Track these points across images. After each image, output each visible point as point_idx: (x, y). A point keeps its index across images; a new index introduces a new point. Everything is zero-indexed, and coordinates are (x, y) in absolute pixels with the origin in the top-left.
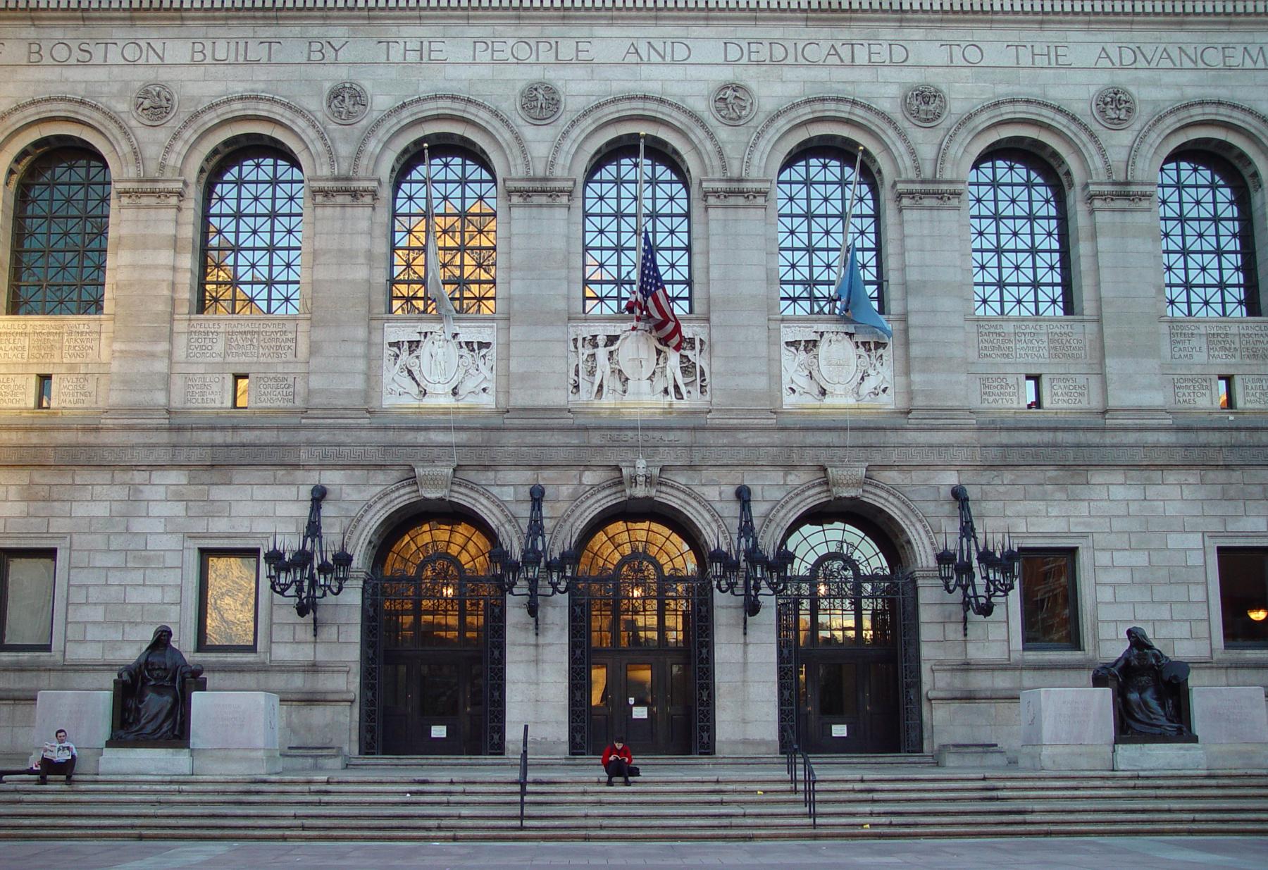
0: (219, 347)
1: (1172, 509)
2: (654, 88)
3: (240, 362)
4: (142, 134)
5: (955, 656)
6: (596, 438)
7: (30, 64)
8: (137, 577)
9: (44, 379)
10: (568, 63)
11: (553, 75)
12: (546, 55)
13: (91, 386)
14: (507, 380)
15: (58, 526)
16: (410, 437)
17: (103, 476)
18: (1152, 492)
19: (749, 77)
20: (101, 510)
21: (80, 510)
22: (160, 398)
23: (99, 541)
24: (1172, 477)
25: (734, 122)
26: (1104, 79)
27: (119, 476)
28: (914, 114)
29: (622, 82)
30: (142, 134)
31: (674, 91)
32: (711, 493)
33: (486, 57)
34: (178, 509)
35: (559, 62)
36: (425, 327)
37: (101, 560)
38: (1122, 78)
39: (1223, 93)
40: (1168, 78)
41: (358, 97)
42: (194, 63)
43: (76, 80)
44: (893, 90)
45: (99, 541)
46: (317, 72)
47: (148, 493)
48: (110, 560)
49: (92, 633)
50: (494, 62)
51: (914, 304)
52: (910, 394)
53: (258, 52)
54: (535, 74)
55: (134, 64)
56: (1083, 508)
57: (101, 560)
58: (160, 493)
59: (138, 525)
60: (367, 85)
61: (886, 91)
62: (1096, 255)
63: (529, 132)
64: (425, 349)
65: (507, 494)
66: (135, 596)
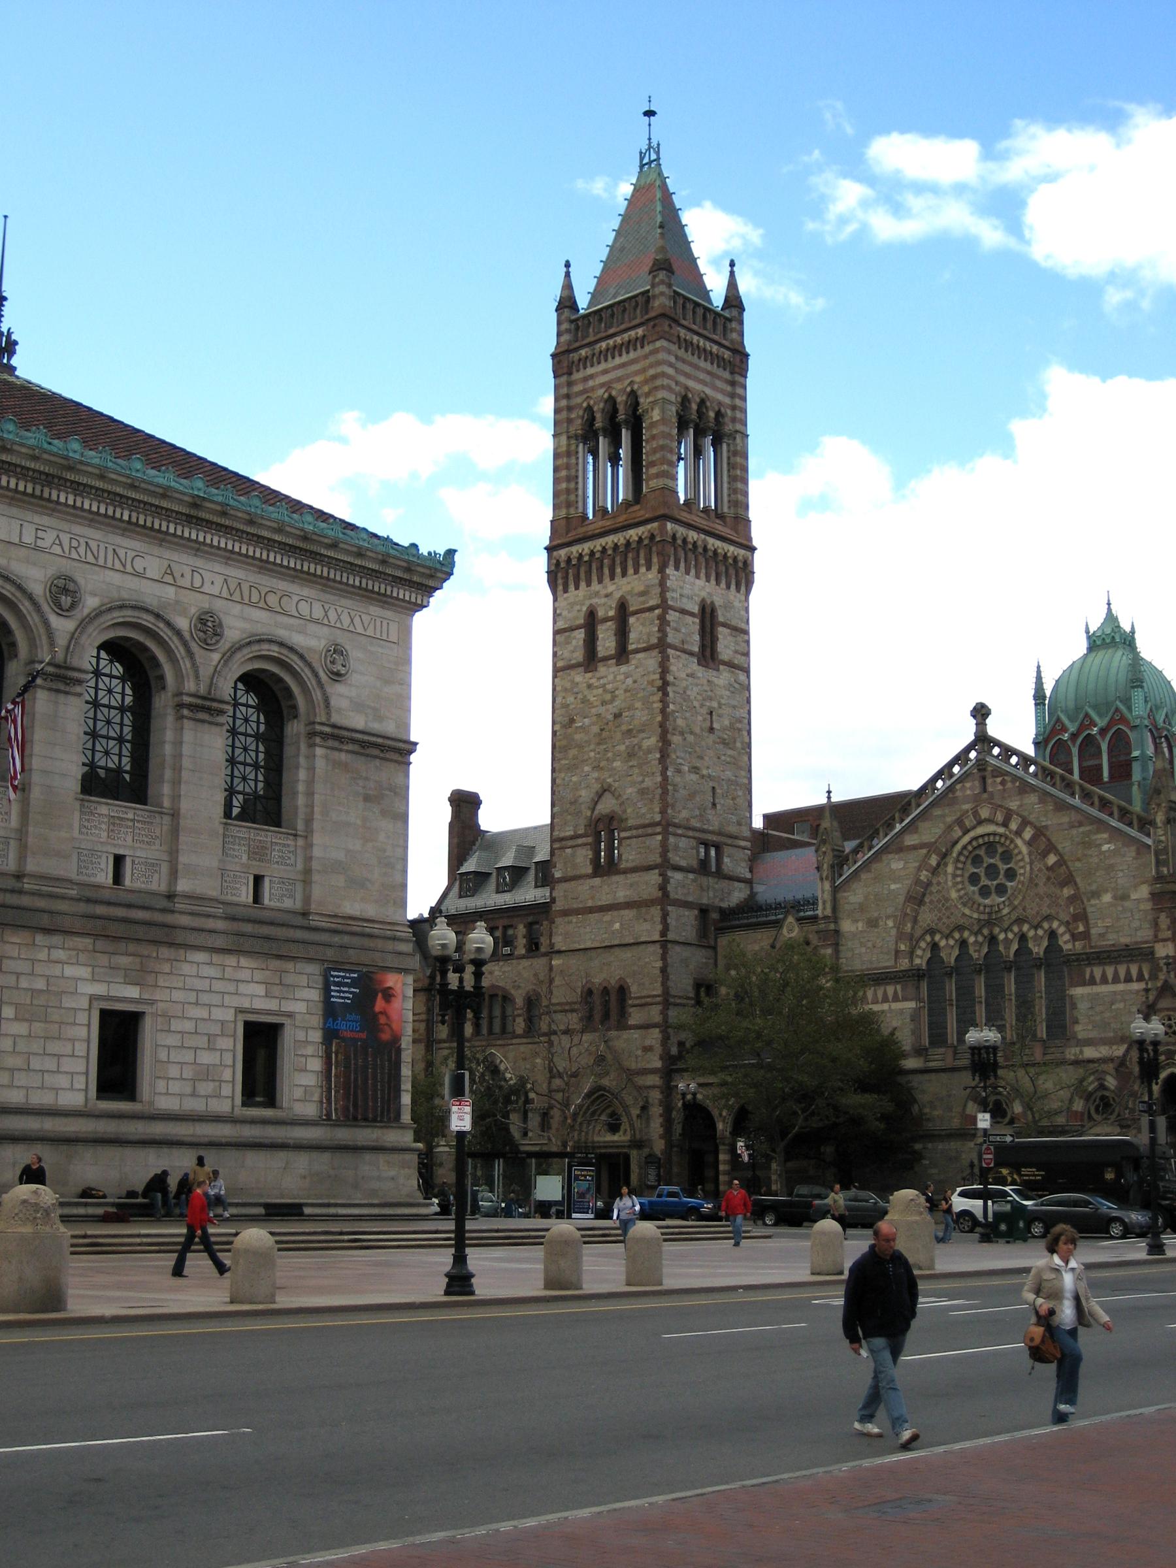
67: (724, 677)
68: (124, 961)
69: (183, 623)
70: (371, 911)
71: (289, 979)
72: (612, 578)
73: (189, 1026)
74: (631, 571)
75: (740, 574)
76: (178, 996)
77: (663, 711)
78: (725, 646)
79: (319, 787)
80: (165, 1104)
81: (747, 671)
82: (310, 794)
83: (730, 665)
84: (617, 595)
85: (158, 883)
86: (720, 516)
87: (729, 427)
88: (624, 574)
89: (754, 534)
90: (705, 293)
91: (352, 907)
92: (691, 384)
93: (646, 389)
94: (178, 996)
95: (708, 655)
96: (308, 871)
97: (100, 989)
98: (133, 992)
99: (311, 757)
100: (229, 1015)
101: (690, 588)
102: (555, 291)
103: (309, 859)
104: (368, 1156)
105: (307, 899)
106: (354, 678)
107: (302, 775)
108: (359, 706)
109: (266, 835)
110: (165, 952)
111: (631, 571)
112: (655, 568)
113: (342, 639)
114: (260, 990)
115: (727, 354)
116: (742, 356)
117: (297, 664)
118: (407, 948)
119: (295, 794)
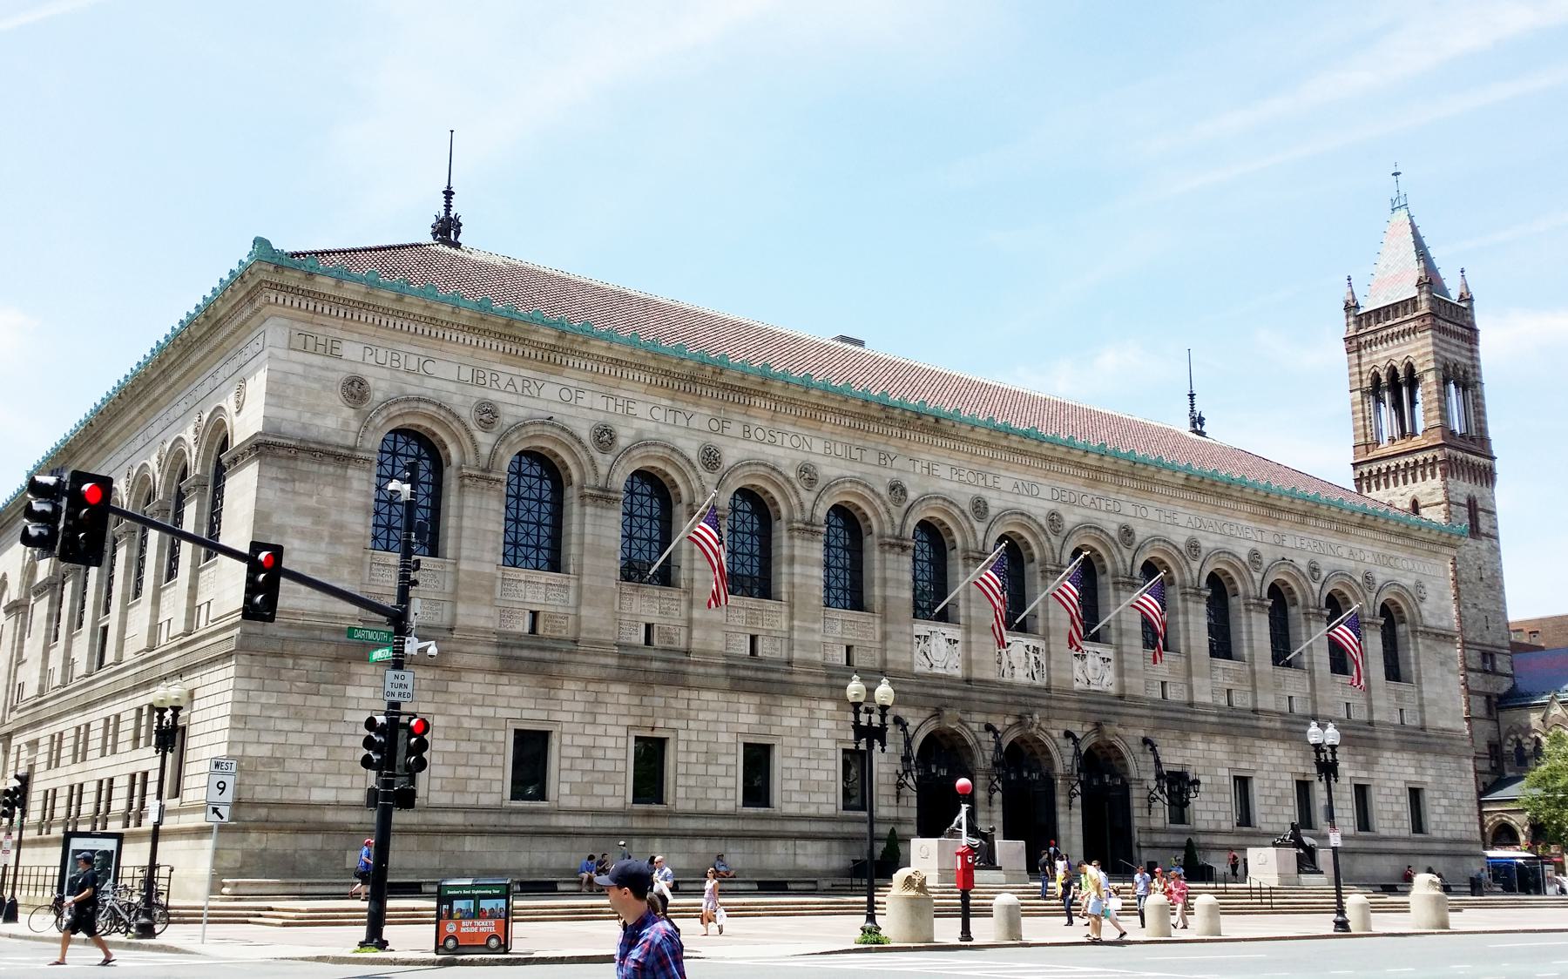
0: (839, 628)
1: (1220, 756)
2: (1024, 508)
3: (850, 638)
4: (803, 494)
5: (1146, 825)
6: (1009, 699)
7: (744, 438)
8: (814, 764)
9: (753, 639)
10: (990, 488)
11: (985, 494)
12: (982, 483)
13: (778, 645)
14: (968, 663)
15: (775, 731)
16: (934, 691)
17: (796, 702)
18: (1212, 746)
19: (1062, 509)
20: (795, 723)
21: (786, 722)
22: (818, 657)
23: (795, 741)
24: (1218, 739)
25: (1056, 533)
26: (1189, 533)
27: (806, 703)
28: (1123, 540)
29: (1011, 502)
30: (803, 494)
31: (1034, 511)
32: (1055, 733)
33: (956, 477)
34: (832, 725)
35: (986, 487)
36: (932, 628)
37: (796, 753)
38: (1197, 533)
39: (1229, 548)
40: (1212, 536)
41: (904, 491)
42: (825, 455)
43: (770, 453)
44: (1115, 526)
45: (795, 741)
46: (882, 471)
47: (818, 714)
48: (803, 754)
49: (795, 797)
50: (960, 481)
51: (1125, 641)
52: (1122, 686)
53: (856, 454)
54: (977, 491)
55: (796, 448)
56: (1188, 753)
57: (796, 753)
58: (823, 714)
59: (814, 733)
60: (906, 484)
61: (1112, 526)
62: (1186, 623)
63: (975, 524)
64: (933, 641)
65: (975, 727)
66: (815, 776)
67: (1484, 544)
68: (1360, 758)
69: (1359, 579)
70: (1450, 725)
71: (1424, 764)
72: (1405, 483)
73: (1387, 791)
74: (1419, 478)
75: (1487, 476)
76: (1382, 776)
77: (1455, 571)
78: (1484, 525)
79: (1422, 660)
80: (1384, 832)
81: (1496, 538)
82: (1417, 664)
83: (1488, 535)
84: (1410, 495)
85: (1364, 717)
86: (1472, 439)
87: (1472, 379)
88: (1415, 481)
89: (1493, 448)
90: (1445, 292)
91: (1441, 724)
92: (1448, 355)
93: (1420, 361)
94: (1382, 776)
95: (1475, 531)
96: (1421, 705)
97: (1351, 774)
98: (1363, 774)
99: (1416, 643)
100: (1402, 785)
101: (1464, 488)
102: (1343, 294)
103: (1421, 699)
104: (1466, 859)
105: (1423, 720)
106: (1429, 599)
107: (1412, 653)
108: (1432, 614)
109: (1402, 687)
110: (1374, 753)
111: (1419, 478)
112: (1439, 476)
113: (1422, 579)
114: (1412, 770)
115: (1466, 332)
116: (1473, 330)
117: (1406, 595)
118: (1467, 744)
119: (1409, 664)
